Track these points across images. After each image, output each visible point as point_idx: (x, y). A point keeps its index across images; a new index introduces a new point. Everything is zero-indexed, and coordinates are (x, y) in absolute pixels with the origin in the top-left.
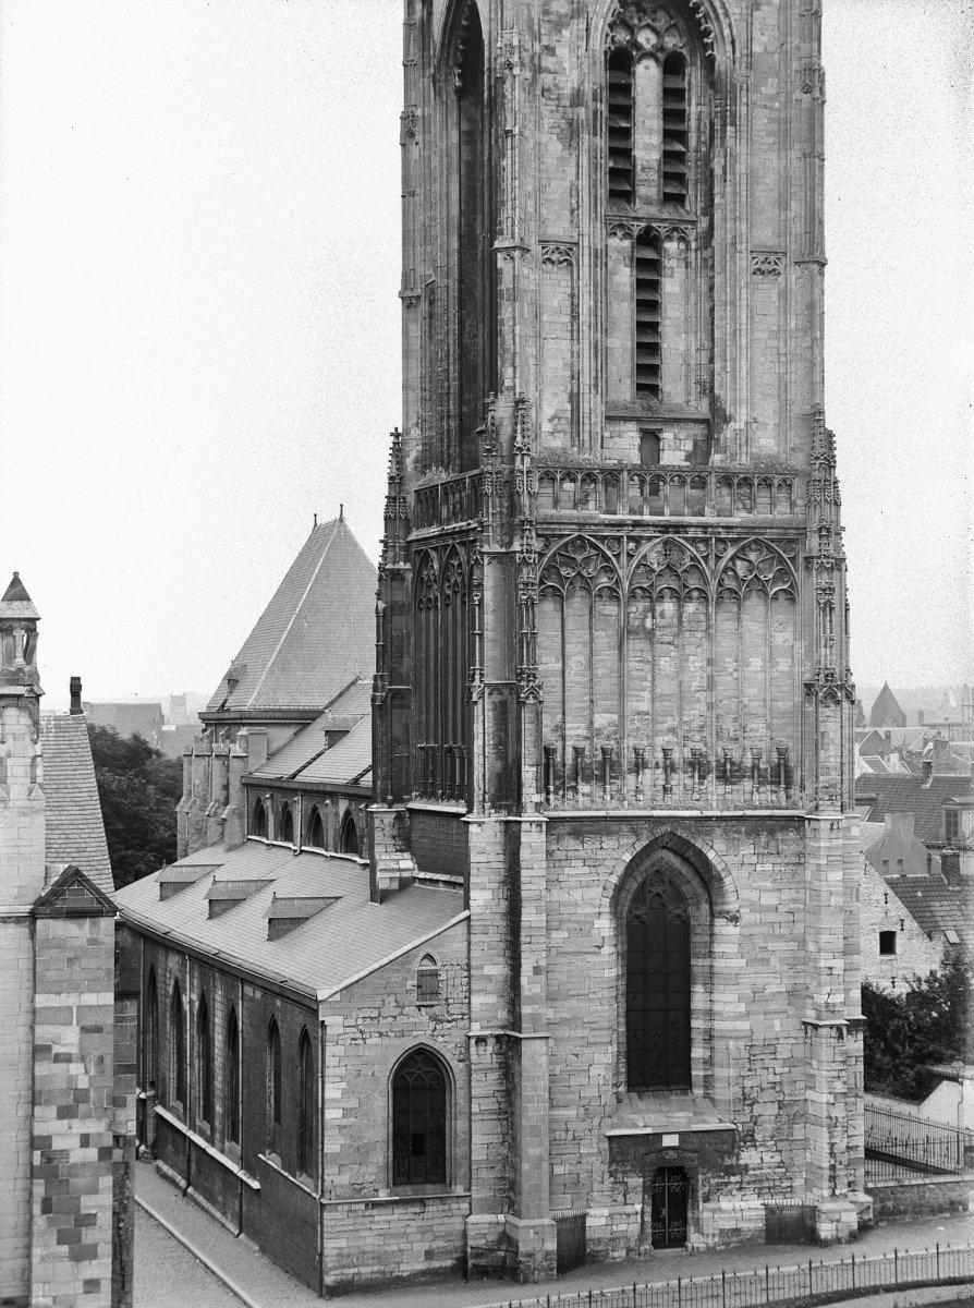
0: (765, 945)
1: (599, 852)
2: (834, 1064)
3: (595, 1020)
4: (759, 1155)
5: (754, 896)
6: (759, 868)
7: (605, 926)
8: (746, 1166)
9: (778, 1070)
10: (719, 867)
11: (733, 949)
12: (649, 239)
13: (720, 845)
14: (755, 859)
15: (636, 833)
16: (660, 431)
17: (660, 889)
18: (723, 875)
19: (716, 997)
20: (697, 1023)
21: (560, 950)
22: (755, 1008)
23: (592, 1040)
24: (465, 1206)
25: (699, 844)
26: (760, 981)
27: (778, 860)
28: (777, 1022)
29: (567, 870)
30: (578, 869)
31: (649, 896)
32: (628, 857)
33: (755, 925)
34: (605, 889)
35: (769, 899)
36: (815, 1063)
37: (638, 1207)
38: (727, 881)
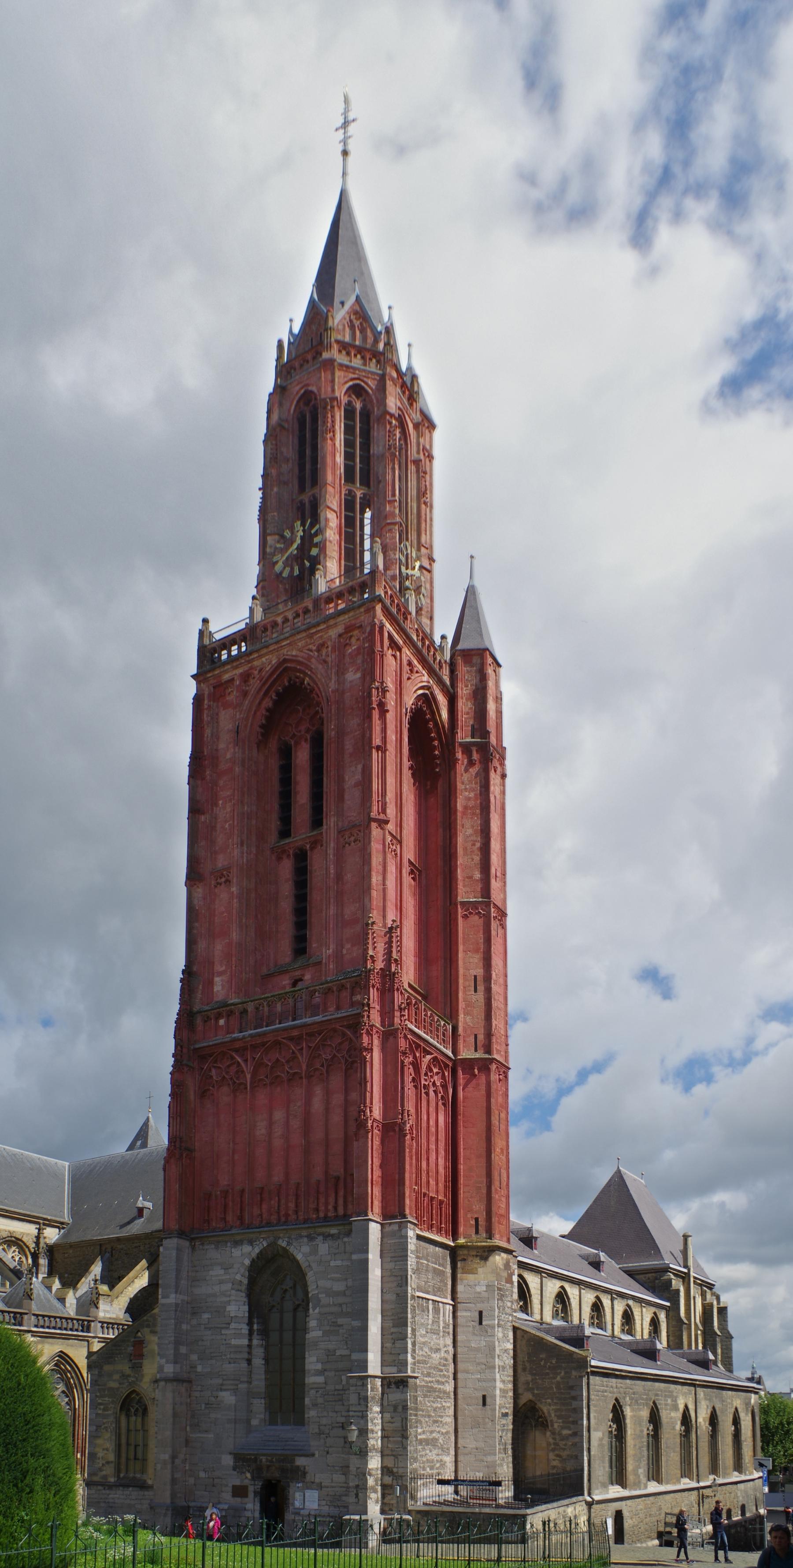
7: (238, 1308)
16: (303, 975)
23: (224, 1387)
29: (211, 1273)
30: (217, 1272)
32: (247, 1262)
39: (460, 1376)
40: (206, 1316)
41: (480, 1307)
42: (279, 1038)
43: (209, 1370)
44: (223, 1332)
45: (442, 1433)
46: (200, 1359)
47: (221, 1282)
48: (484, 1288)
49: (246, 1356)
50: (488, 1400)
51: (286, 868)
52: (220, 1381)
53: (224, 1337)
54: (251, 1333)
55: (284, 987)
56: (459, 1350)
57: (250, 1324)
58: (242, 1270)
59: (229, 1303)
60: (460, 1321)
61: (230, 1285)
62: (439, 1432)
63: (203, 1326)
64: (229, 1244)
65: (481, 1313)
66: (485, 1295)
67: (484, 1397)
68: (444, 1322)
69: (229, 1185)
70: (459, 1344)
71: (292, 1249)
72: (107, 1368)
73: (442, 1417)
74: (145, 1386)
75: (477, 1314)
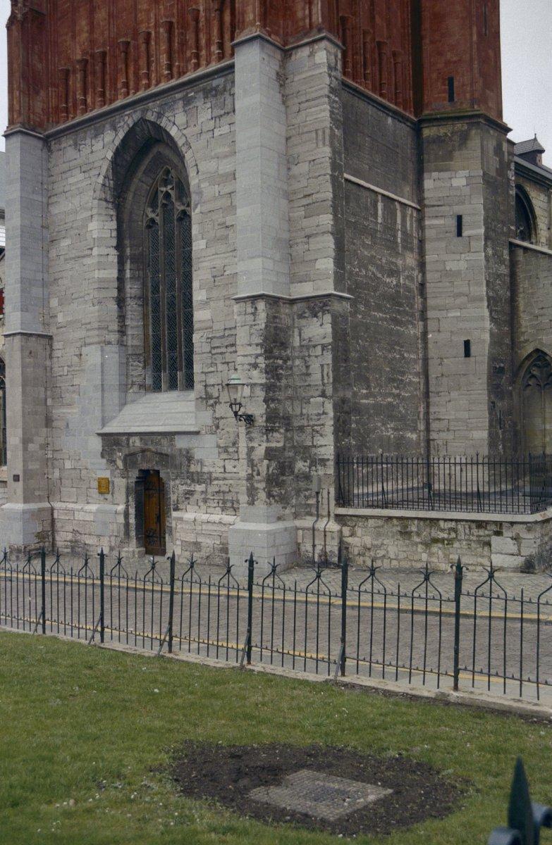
0: (223, 220)
1: (90, 156)
2: (249, 348)
3: (88, 321)
4: (222, 463)
6: (217, 132)
8: (210, 473)
13: (180, 118)
18: (184, 149)
21: (67, 257)
22: (215, 294)
23: (88, 341)
26: (218, 263)
32: (110, 155)
34: (95, 192)
37: (121, 508)
39: (430, 314)
41: (458, 209)
45: (404, 399)
46: (61, 304)
48: (464, 182)
49: (115, 293)
50: (473, 349)
54: (121, 262)
56: (429, 276)
57: (119, 247)
60: (429, 233)
61: (91, 193)
62: (398, 395)
65: (459, 218)
66: (467, 190)
67: (467, 344)
68: (404, 233)
70: (428, 267)
71: (163, 123)
73: (403, 373)
75: (454, 222)
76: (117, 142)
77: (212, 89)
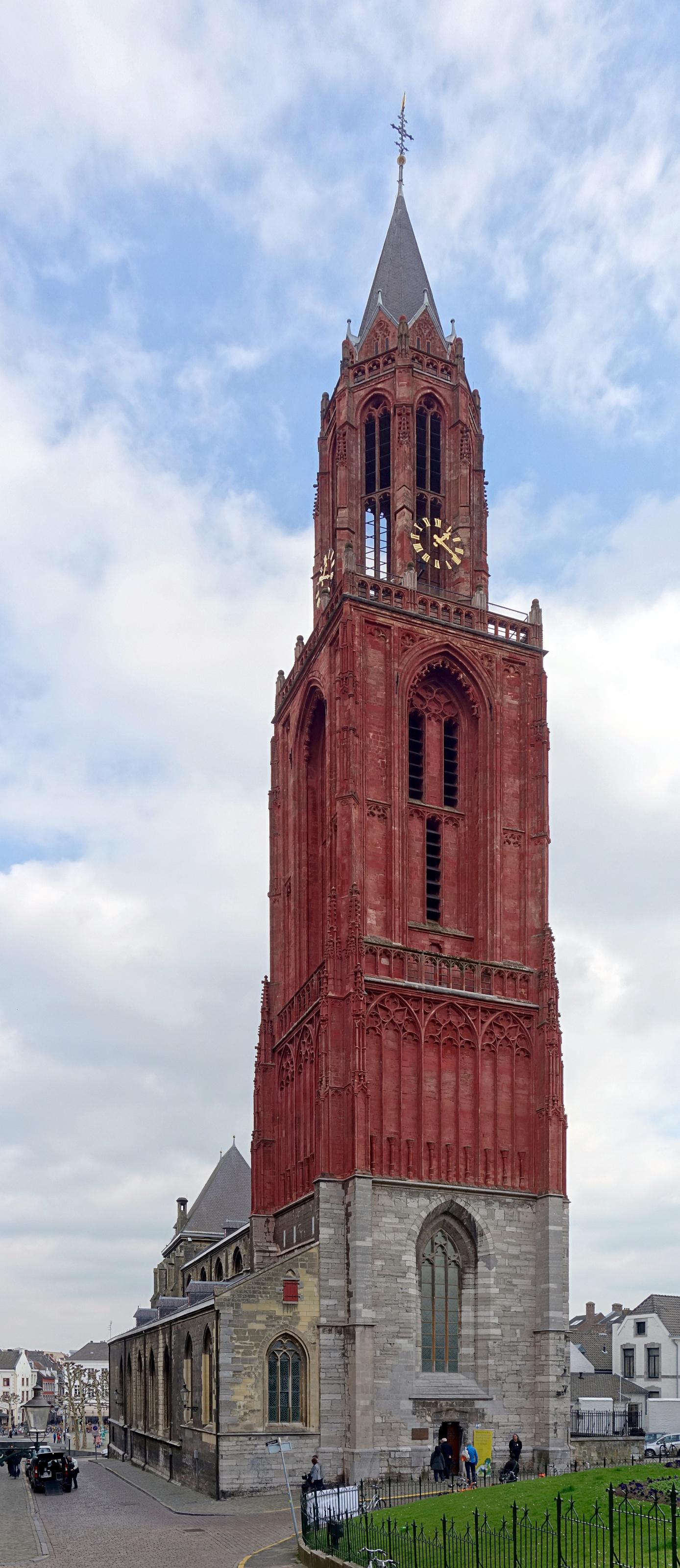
5: (504, 1247)
9: (519, 1363)
10: (483, 1226)
11: (492, 1281)
12: (433, 824)
13: (483, 1212)
14: (504, 1223)
15: (428, 1197)
16: (442, 942)
17: (443, 1242)
19: (480, 1313)
20: (466, 1331)
22: (504, 1320)
24: (315, 1441)
25: (470, 1210)
26: (507, 1303)
27: (520, 1225)
28: (518, 1331)
29: (384, 1219)
30: (389, 1220)
31: (435, 1247)
32: (424, 1215)
33: (504, 1266)
35: (513, 1250)
36: (543, 1358)
38: (488, 1235)
40: (379, 1263)
42: (455, 1002)
43: (384, 1317)
44: (399, 1280)
47: (395, 1231)
51: (418, 829)
52: (397, 1329)
53: (400, 1286)
55: (423, 947)
58: (420, 1223)
59: (404, 1252)
63: (375, 1273)
64: (404, 1194)
69: (395, 1133)
72: (245, 1307)
74: (303, 1330)
76: (431, 1210)
77: (505, 1203)
